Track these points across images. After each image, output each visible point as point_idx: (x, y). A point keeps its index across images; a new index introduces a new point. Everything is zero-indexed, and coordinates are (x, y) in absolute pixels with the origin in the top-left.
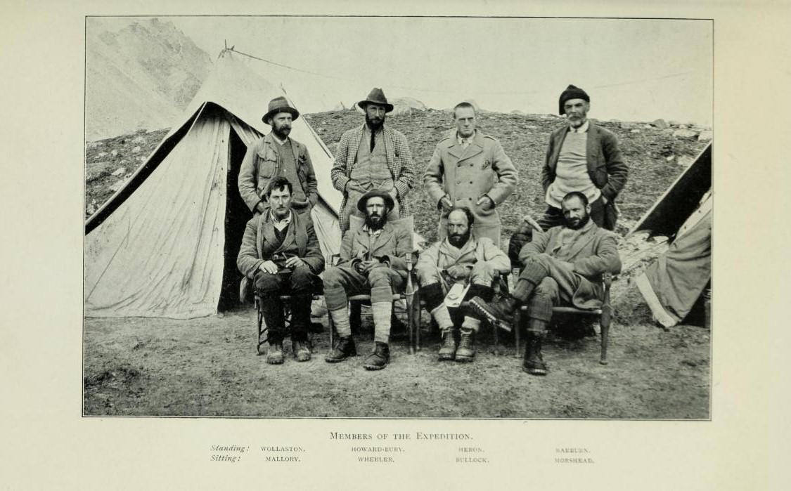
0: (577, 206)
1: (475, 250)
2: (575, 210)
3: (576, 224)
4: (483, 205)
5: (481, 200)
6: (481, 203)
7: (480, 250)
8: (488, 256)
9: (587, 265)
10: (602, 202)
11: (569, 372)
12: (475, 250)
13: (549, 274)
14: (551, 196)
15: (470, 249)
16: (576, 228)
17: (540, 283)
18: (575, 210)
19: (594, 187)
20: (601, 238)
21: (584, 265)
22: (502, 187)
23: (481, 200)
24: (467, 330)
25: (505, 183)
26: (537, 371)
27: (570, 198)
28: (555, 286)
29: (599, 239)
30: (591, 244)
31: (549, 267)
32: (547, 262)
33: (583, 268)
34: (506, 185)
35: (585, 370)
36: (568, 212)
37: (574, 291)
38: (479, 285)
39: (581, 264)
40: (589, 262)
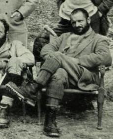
0: (81, 19)
1: (10, 49)
2: (79, 21)
3: (80, 31)
4: (15, 18)
5: (14, 14)
6: (14, 16)
7: (13, 49)
8: (18, 54)
9: (88, 60)
10: (99, 15)
11: (75, 135)
12: (10, 49)
13: (62, 66)
14: (62, 11)
15: (6, 49)
16: (80, 34)
17: (55, 72)
18: (79, 21)
19: (93, 5)
20: (98, 41)
21: (86, 60)
22: (28, 5)
23: (14, 14)
24: (4, 105)
25: (30, 2)
26: (53, 134)
27: (76, 13)
28: (65, 74)
29: (96, 41)
30: (91, 45)
31: (61, 61)
32: (60, 58)
33: (85, 62)
34: (31, 4)
35: (87, 133)
36: (75, 22)
37: (79, 78)
38: (13, 74)
39: (84, 59)
40: (89, 58)
